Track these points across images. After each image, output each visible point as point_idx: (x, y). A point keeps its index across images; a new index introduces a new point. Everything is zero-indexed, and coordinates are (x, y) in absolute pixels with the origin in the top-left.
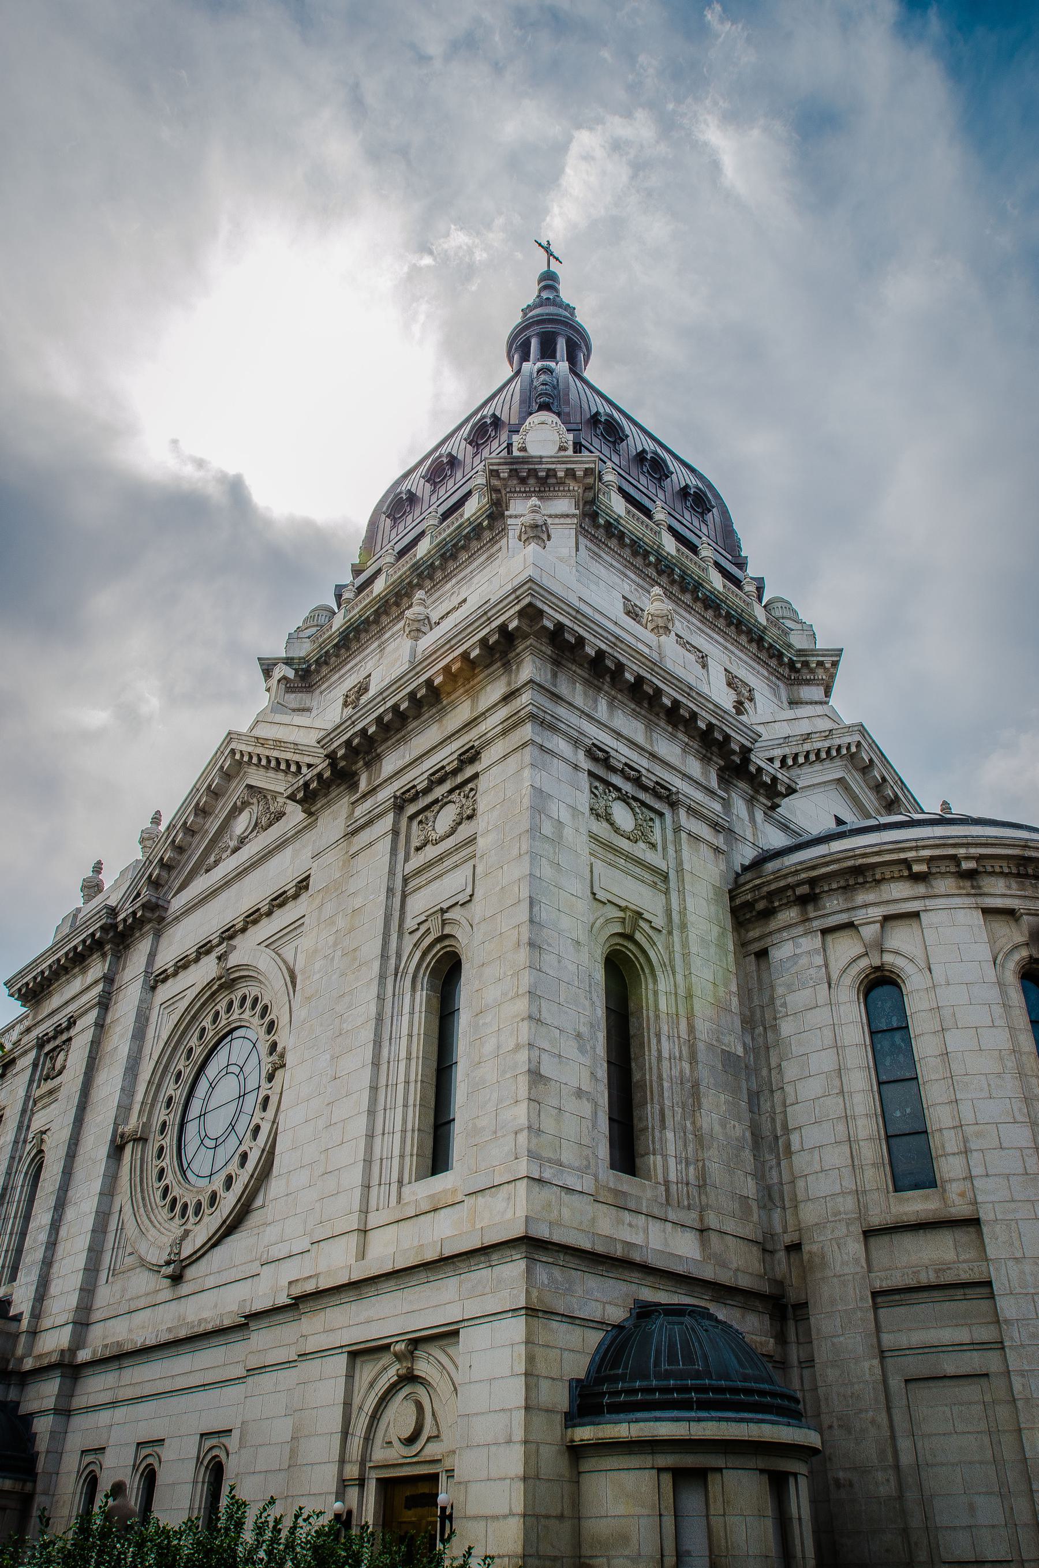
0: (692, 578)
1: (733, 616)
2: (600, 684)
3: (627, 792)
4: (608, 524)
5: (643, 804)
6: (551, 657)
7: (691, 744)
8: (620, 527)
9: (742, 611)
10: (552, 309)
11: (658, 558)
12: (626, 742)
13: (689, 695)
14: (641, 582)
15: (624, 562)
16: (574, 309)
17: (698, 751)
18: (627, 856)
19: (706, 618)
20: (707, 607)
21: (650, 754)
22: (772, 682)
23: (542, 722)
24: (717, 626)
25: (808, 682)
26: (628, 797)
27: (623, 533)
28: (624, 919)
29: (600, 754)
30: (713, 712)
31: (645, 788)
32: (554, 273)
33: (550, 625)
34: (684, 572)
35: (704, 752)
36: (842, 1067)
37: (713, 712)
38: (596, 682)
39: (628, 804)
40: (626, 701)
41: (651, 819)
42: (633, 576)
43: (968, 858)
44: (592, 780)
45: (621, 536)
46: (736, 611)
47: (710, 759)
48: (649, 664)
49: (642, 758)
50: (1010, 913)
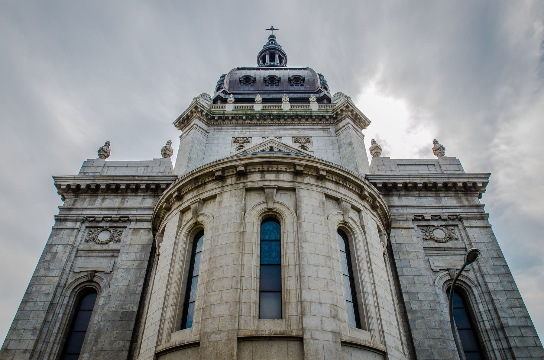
0: (266, 114)
1: (292, 116)
2: (96, 194)
3: (106, 227)
4: (220, 118)
5: (116, 227)
6: (73, 196)
7: (146, 194)
8: (226, 115)
9: (296, 112)
11: (246, 116)
12: (106, 209)
13: (134, 179)
14: (244, 127)
15: (234, 125)
17: (151, 196)
18: (99, 251)
19: (281, 123)
20: (279, 120)
21: (118, 208)
22: (325, 129)
23: (60, 220)
24: (287, 123)
25: (342, 120)
27: (228, 116)
28: (87, 275)
29: (90, 219)
30: (148, 179)
34: (261, 114)
35: (153, 194)
37: (148, 179)
38: (94, 195)
39: (108, 230)
40: (109, 194)
42: (239, 128)
45: (227, 118)
46: (293, 114)
48: (112, 178)
49: (114, 211)
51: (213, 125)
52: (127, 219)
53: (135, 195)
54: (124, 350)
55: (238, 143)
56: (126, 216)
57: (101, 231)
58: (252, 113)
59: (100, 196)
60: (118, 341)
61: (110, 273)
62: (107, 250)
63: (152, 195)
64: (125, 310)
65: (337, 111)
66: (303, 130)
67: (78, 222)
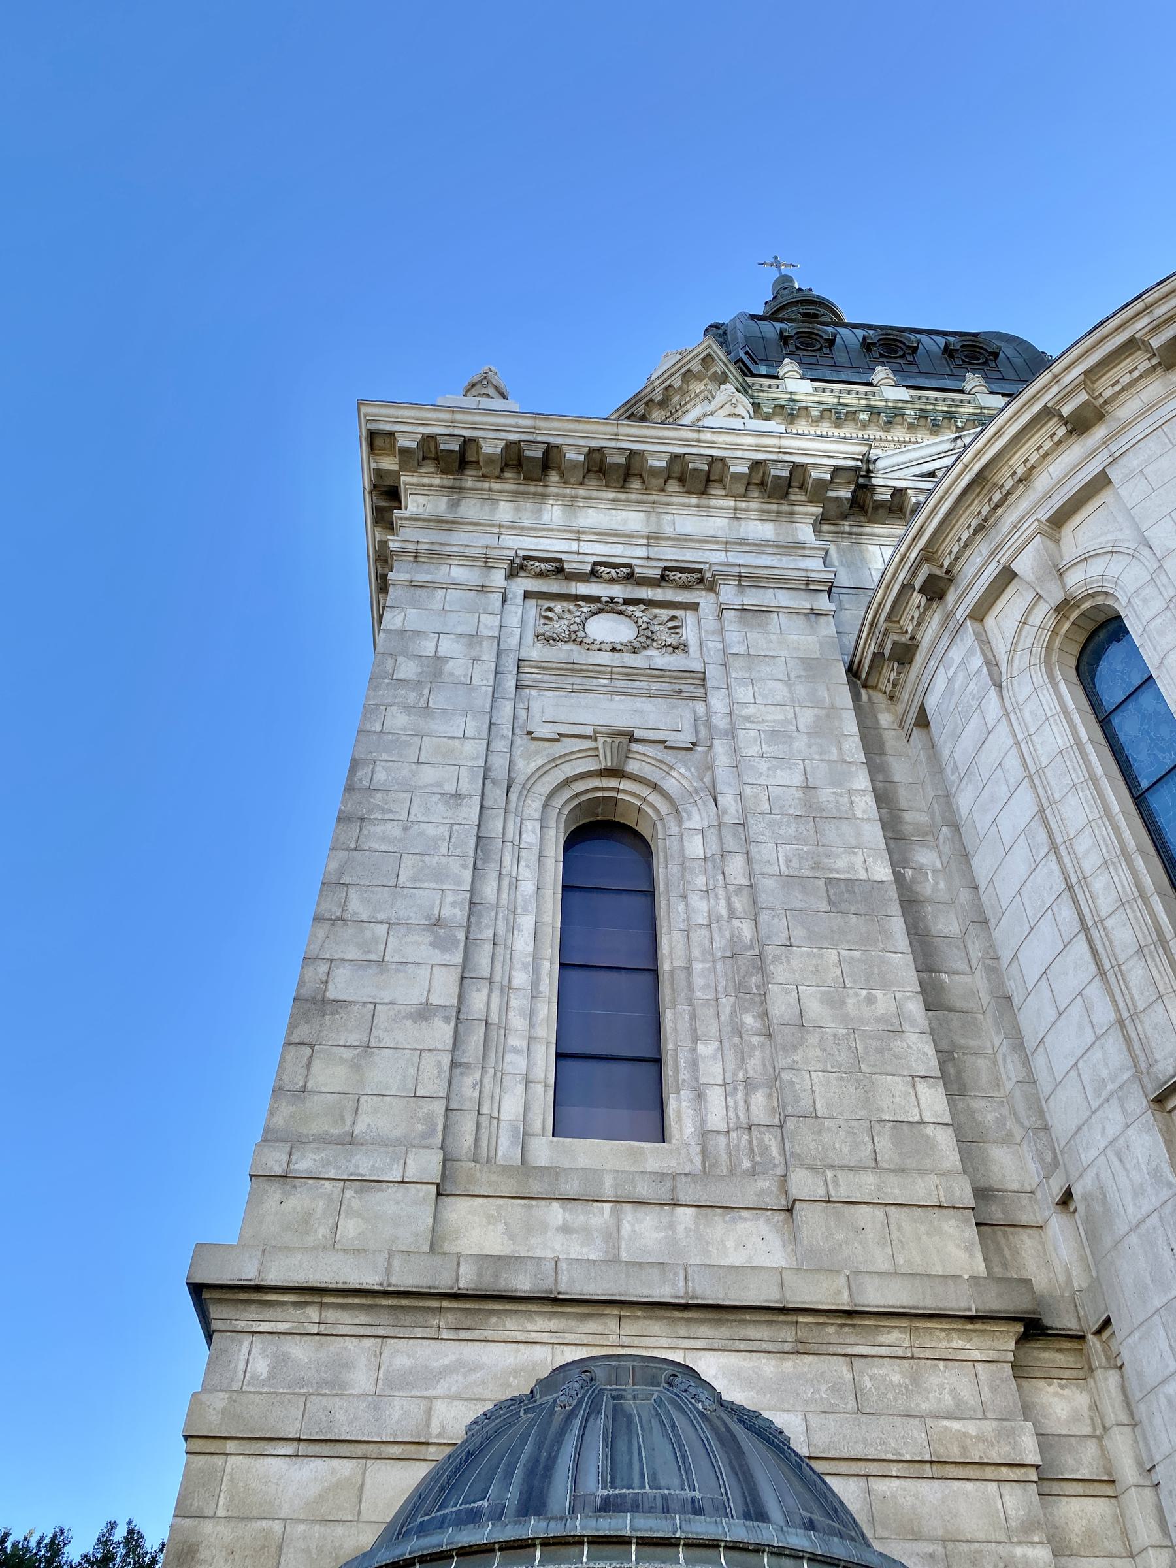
2: (540, 489)
5: (650, 603)
7: (744, 505)
17: (763, 511)
32: (786, 276)
36: (1045, 804)
41: (673, 618)
47: (792, 513)
53: (698, 506)
54: (906, 1027)
59: (556, 495)
60: (864, 992)
61: (691, 749)
63: (769, 512)
64: (837, 876)
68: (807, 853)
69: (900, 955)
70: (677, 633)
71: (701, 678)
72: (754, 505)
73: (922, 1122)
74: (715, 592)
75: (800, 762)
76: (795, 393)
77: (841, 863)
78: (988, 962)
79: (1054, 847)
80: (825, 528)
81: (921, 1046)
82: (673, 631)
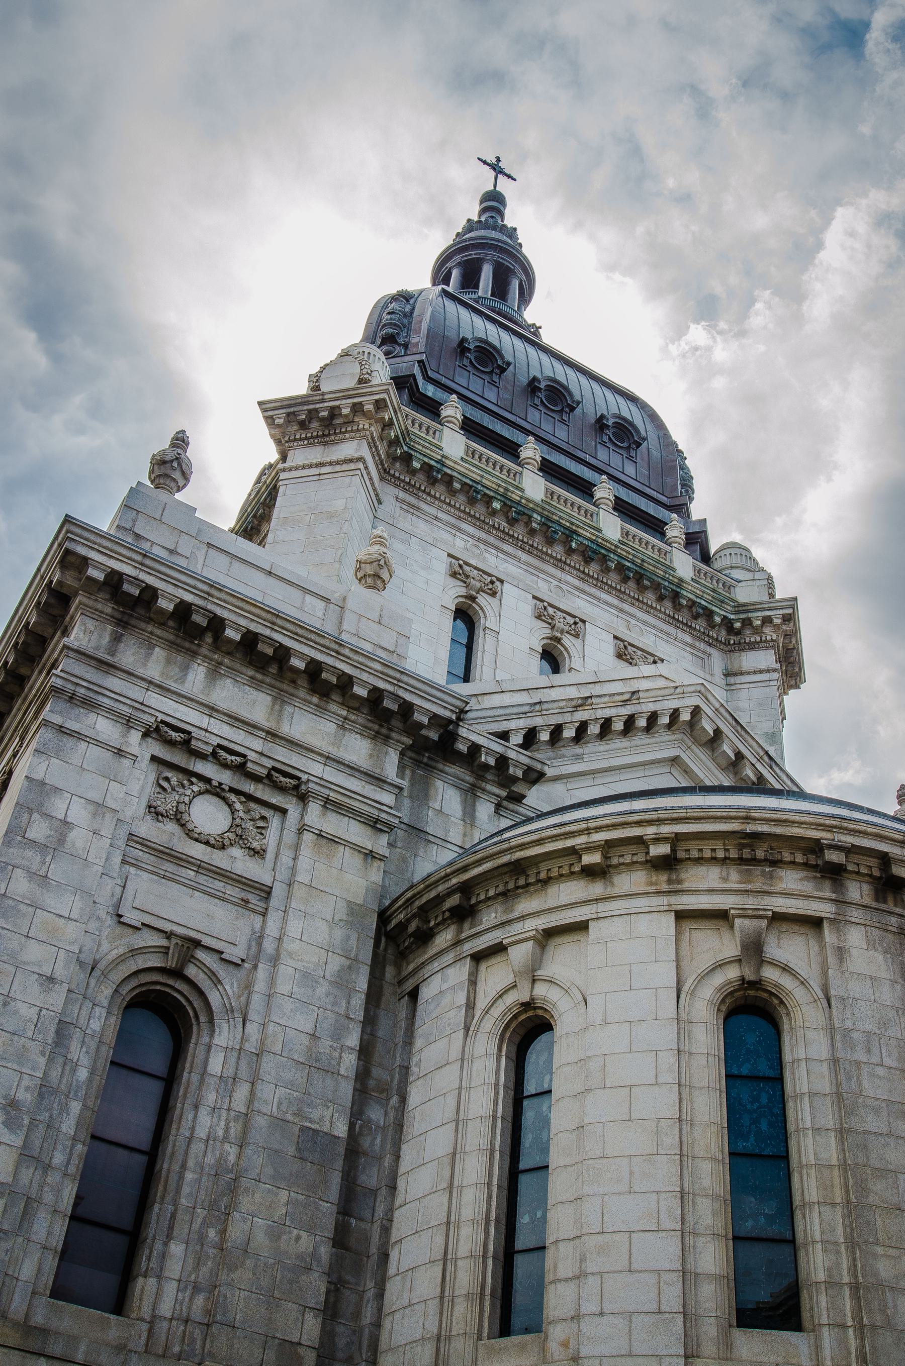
0: (560, 525)
1: (629, 569)
2: (194, 647)
3: (220, 784)
4: (427, 469)
5: (250, 798)
6: (112, 617)
7: (353, 717)
8: (445, 469)
9: (643, 561)
10: (493, 234)
11: (505, 504)
12: (225, 718)
13: (338, 652)
14: (484, 536)
15: (457, 512)
16: (515, 229)
17: (366, 727)
18: (199, 866)
19: (588, 575)
20: (588, 560)
21: (268, 733)
22: (699, 650)
23: (71, 698)
24: (606, 584)
25: (753, 646)
26: (223, 790)
27: (451, 476)
28: (168, 948)
29: (174, 735)
31: (255, 778)
33: (100, 576)
34: (548, 518)
35: (376, 727)
36: (459, 1150)
37: (382, 673)
38: (187, 645)
39: (224, 799)
40: (238, 666)
41: (263, 818)
42: (470, 529)
43: (658, 840)
44: (161, 768)
45: (448, 480)
46: (633, 562)
48: (269, 617)
49: (251, 738)
50: (721, 916)
51: (397, 482)
52: (293, 782)
53: (316, 705)
54: (314, 1267)
55: (465, 582)
56: (290, 770)
57: (200, 793)
58: (523, 501)
59: (205, 656)
60: (296, 1232)
61: (237, 965)
62: (228, 874)
63: (370, 729)
64: (309, 1125)
65: (750, 615)
66: (641, 625)
67: (133, 732)
68: (296, 1099)
69: (329, 1205)
70: (262, 834)
71: (266, 893)
72: (360, 720)
73: (299, 1344)
74: (304, 801)
75: (316, 1008)
76: (446, 458)
77: (315, 1115)
78: (385, 1222)
79: (451, 1186)
80: (409, 753)
81: (318, 1283)
82: (259, 831)
